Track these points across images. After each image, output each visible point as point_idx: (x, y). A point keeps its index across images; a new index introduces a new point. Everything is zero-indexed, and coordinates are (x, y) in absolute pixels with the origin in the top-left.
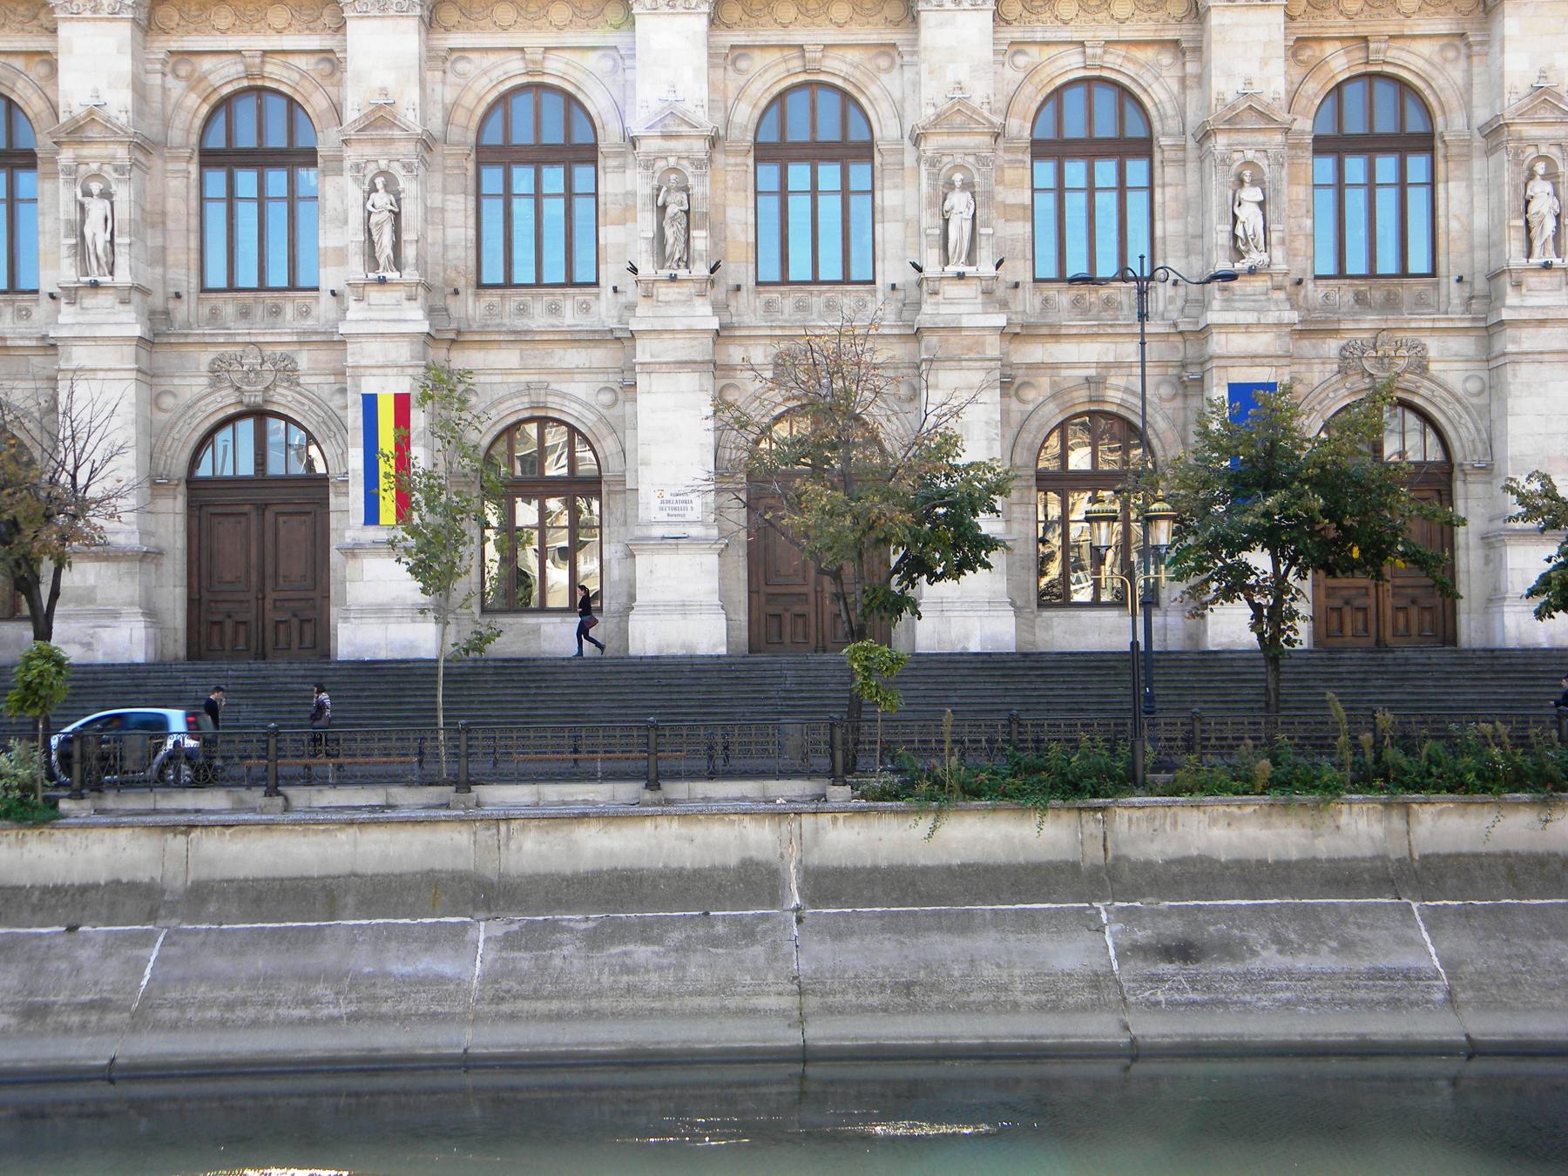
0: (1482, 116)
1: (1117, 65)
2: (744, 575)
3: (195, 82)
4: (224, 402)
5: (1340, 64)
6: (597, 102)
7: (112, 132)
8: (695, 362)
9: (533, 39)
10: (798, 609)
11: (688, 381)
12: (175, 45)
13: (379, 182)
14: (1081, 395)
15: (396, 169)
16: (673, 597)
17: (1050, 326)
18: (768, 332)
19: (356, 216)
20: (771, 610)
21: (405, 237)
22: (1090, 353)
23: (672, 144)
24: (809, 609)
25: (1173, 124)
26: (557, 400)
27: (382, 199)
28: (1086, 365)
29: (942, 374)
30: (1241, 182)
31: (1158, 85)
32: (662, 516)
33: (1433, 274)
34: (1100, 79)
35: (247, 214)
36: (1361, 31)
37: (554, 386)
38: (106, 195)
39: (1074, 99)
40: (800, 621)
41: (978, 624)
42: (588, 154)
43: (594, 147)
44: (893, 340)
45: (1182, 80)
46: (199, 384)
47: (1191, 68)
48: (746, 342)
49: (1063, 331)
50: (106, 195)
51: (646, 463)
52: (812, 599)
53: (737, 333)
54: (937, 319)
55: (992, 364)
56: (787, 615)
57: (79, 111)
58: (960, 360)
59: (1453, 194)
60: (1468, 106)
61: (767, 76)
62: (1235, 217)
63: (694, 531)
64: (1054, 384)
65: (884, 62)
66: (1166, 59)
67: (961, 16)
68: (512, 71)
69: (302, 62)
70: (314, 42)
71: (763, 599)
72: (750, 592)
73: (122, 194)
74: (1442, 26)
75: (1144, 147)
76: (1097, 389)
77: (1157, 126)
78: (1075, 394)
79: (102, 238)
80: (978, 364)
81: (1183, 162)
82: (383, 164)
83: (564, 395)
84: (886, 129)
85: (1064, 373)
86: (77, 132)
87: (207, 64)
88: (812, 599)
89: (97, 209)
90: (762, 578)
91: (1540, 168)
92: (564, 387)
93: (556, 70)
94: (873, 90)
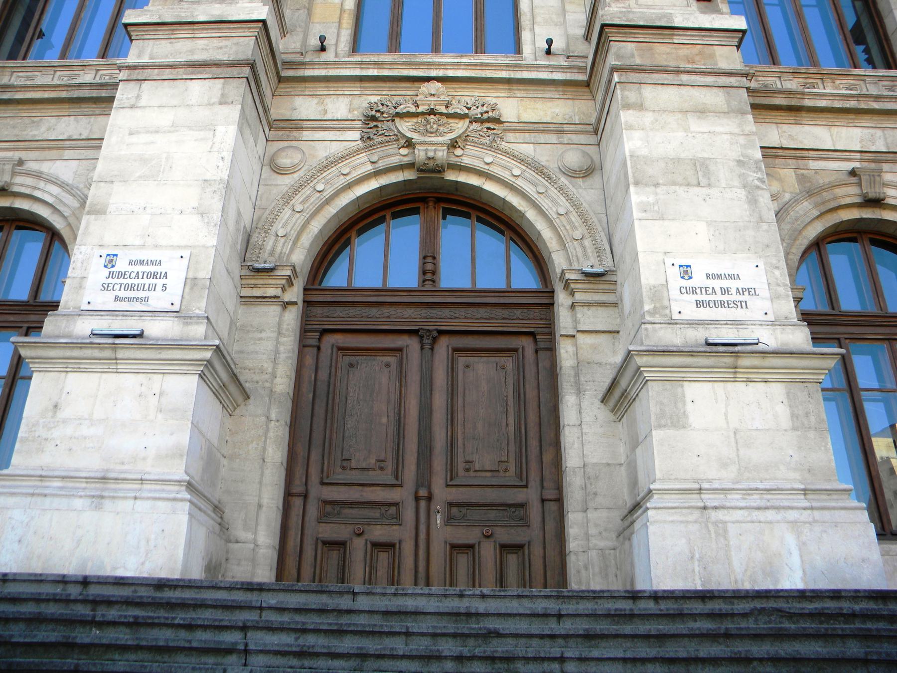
2: (276, 453)
8: (218, 64)
10: (379, 533)
11: (199, 90)
14: (850, 193)
16: (89, 462)
18: (357, 72)
20: (328, 531)
22: (851, 136)
24: (402, 534)
26: (29, 181)
29: (648, 92)
32: (105, 300)
37: (32, 166)
40: (383, 558)
41: (791, 540)
44: (551, 92)
48: (321, 89)
49: (808, 103)
51: (100, 211)
52: (408, 514)
53: (308, 73)
54: (631, 16)
55: (733, 80)
56: (358, 547)
58: (678, 72)
63: (156, 328)
64: (801, 179)
71: (313, 511)
72: (288, 495)
76: (872, 183)
78: (839, 191)
80: (709, 80)
83: (38, 175)
85: (813, 165)
88: (408, 514)
90: (314, 478)
92: (46, 167)
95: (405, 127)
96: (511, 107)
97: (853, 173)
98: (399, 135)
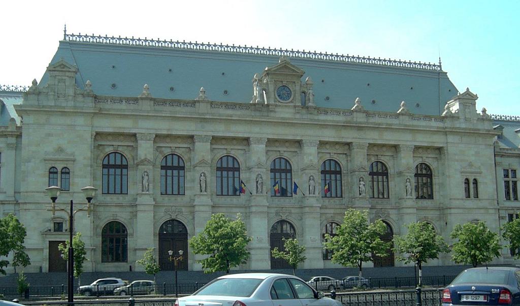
0: (397, 170)
1: (335, 157)
3: (161, 152)
4: (167, 218)
5: (373, 159)
6: (241, 159)
7: (149, 161)
9: (228, 147)
12: (158, 145)
13: (202, 175)
15: (206, 172)
17: (325, 206)
19: (197, 181)
21: (207, 185)
22: (332, 211)
23: (259, 169)
25: (346, 169)
27: (203, 177)
28: (331, 214)
30: (360, 181)
31: (342, 161)
33: (388, 198)
34: (332, 160)
35: (176, 179)
36: (377, 154)
38: (147, 175)
39: (327, 163)
42: (238, 169)
43: (239, 168)
45: (347, 161)
46: (162, 214)
47: (349, 158)
50: (147, 175)
57: (143, 158)
59: (391, 184)
60: (394, 167)
61: (274, 156)
62: (360, 187)
65: (294, 154)
66: (345, 155)
67: (312, 148)
68: (224, 153)
69: (184, 149)
73: (151, 175)
74: (390, 154)
75: (340, 173)
77: (342, 169)
79: (147, 184)
81: (348, 176)
82: (203, 171)
84: (294, 167)
85: (328, 215)
86: (142, 162)
87: (163, 149)
89: (146, 178)
91: (408, 180)
93: (233, 153)
94: (293, 160)
95: (281, 214)
96: (293, 211)
97: (332, 216)
98: (280, 215)
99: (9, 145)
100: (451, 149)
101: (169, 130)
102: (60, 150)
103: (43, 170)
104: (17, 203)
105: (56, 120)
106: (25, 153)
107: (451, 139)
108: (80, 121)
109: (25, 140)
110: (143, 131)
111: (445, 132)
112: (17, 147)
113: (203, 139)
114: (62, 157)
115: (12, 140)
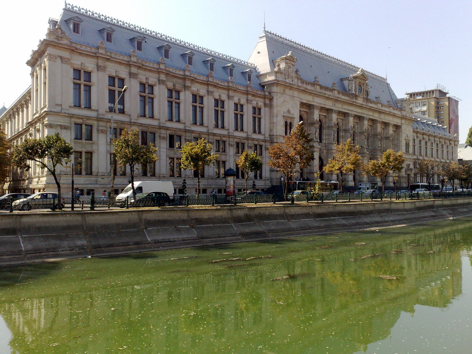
70: (325, 114)
99: (265, 105)
100: (403, 127)
101: (324, 105)
102: (289, 111)
103: (282, 123)
104: (272, 142)
105: (288, 91)
106: (275, 111)
107: (403, 121)
108: (296, 93)
109: (275, 102)
110: (316, 104)
111: (403, 118)
112: (271, 106)
113: (335, 112)
114: (290, 115)
115: (267, 101)
